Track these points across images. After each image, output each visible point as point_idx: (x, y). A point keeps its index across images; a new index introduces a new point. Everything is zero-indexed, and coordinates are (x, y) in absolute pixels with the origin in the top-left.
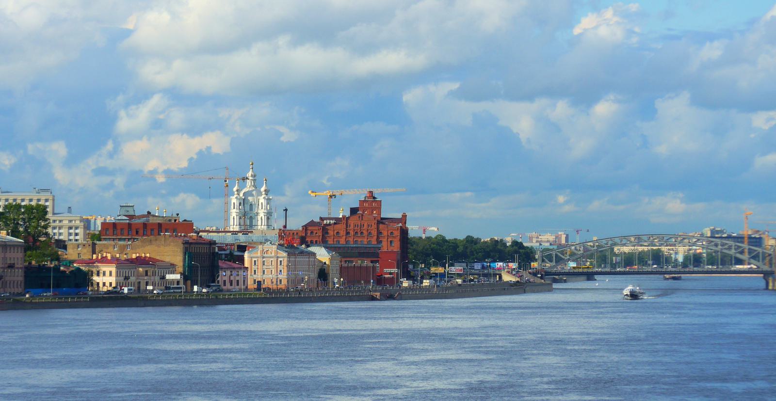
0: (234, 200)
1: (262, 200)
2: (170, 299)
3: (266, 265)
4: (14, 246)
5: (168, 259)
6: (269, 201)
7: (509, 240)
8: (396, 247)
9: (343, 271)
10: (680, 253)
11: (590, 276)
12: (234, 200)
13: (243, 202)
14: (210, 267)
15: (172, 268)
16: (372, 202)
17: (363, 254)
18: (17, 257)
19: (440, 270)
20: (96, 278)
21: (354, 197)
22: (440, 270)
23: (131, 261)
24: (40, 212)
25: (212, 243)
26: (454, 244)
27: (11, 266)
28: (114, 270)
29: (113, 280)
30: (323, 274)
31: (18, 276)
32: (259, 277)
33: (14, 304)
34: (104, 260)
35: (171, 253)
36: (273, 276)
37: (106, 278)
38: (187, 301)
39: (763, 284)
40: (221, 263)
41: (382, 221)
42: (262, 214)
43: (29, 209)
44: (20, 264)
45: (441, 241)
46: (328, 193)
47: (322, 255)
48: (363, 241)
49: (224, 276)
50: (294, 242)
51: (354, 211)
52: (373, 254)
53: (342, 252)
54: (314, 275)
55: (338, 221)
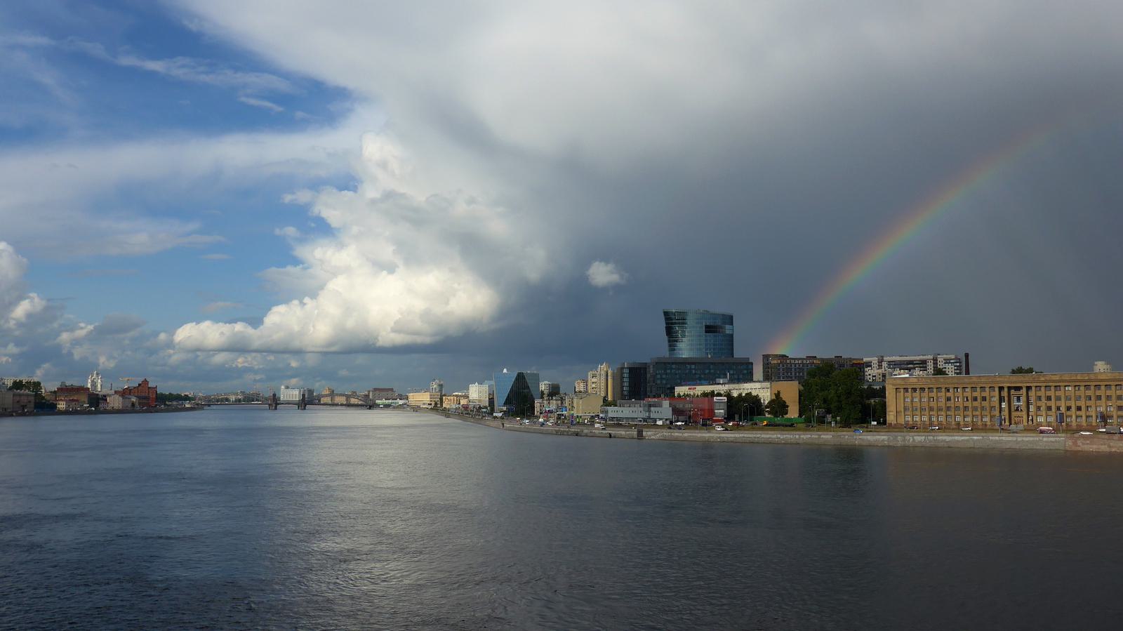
0: (89, 381)
1: (99, 381)
3: (115, 402)
4: (31, 395)
5: (83, 400)
6: (101, 381)
7: (183, 395)
8: (154, 396)
9: (139, 404)
10: (233, 398)
11: (209, 405)
12: (89, 381)
13: (92, 381)
14: (96, 402)
15: (84, 402)
16: (146, 382)
17: (145, 398)
18: (33, 398)
19: (170, 403)
20: (58, 406)
21: (140, 380)
22: (170, 403)
23: (70, 400)
25: (98, 395)
26: (165, 395)
27: (30, 402)
28: (65, 403)
29: (64, 406)
30: (133, 405)
32: (112, 405)
33: (30, 414)
34: (61, 400)
35: (84, 398)
36: (117, 405)
37: (62, 406)
38: (90, 413)
39: (268, 408)
40: (101, 401)
41: (149, 388)
42: (99, 386)
43: (34, 383)
44: (33, 401)
46: (126, 379)
48: (143, 395)
49: (101, 406)
50: (124, 393)
51: (139, 385)
54: (130, 405)
55: (135, 388)
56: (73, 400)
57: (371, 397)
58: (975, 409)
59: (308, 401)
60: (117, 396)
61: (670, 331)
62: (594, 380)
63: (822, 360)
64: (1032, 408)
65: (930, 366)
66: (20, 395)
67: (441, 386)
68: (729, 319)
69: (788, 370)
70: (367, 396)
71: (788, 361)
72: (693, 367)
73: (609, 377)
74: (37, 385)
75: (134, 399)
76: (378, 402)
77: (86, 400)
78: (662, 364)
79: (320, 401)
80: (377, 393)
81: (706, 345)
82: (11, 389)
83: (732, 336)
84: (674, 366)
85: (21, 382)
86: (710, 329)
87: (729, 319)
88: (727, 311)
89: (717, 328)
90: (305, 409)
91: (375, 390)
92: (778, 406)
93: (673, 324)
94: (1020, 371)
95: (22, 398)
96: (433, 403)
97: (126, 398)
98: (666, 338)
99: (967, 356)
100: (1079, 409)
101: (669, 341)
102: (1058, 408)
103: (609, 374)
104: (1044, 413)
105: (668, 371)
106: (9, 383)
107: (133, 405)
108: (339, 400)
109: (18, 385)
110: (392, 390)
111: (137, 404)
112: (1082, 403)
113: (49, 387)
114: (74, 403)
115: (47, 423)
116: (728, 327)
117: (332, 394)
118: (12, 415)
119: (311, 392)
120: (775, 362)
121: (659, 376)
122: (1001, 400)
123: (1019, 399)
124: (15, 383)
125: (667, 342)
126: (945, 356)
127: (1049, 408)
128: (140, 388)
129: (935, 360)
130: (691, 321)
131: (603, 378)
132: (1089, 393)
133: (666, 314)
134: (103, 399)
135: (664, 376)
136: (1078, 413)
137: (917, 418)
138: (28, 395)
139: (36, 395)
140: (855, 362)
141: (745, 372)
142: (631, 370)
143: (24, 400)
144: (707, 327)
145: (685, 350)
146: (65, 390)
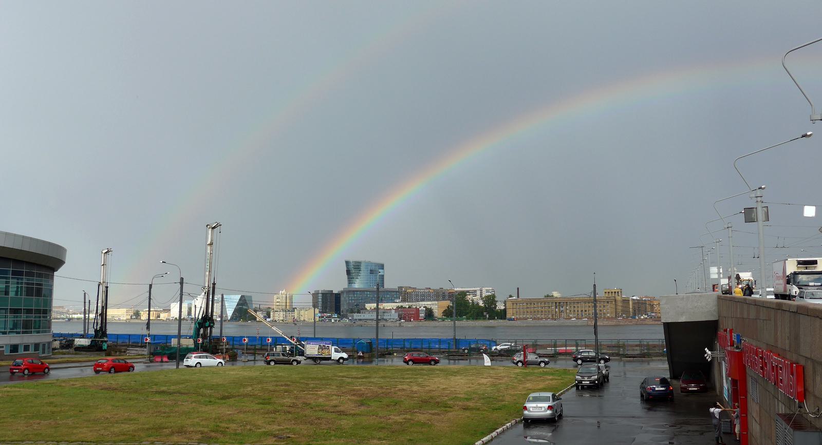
58: (545, 311)
61: (348, 272)
62: (278, 300)
63: (434, 290)
64: (568, 311)
65: (478, 293)
68: (382, 266)
69: (417, 295)
71: (417, 291)
72: (368, 293)
73: (288, 299)
78: (349, 292)
81: (370, 281)
83: (383, 276)
84: (358, 293)
86: (372, 272)
87: (382, 266)
88: (381, 262)
89: (376, 270)
92: (448, 313)
93: (352, 270)
94: (548, 296)
98: (346, 276)
99: (518, 289)
100: (586, 311)
101: (348, 278)
102: (578, 311)
103: (288, 297)
104: (573, 313)
105: (355, 295)
112: (587, 309)
116: (380, 270)
120: (410, 291)
121: (350, 298)
122: (556, 307)
123: (562, 307)
125: (347, 279)
126: (486, 288)
127: (574, 311)
129: (481, 291)
130: (363, 268)
131: (284, 299)
132: (589, 305)
133: (347, 263)
135: (353, 298)
136: (586, 313)
137: (521, 316)
140: (450, 291)
141: (395, 296)
142: (322, 294)
144: (370, 270)
145: (358, 285)
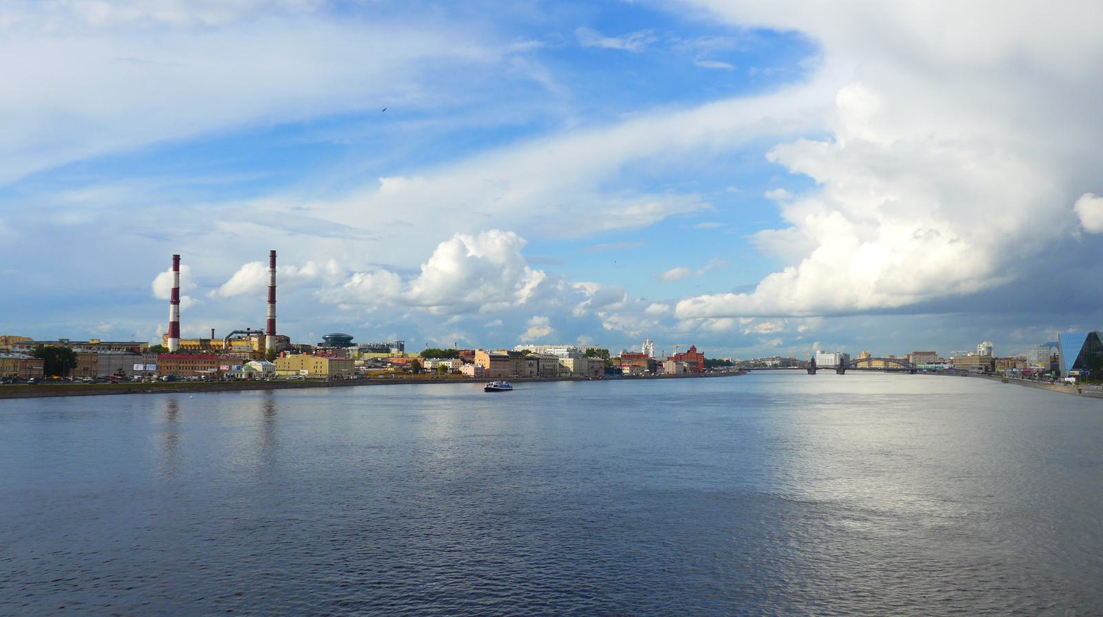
1: (651, 348)
2: (645, 378)
3: (670, 367)
8: (702, 362)
9: (691, 369)
11: (749, 370)
13: (646, 349)
14: (654, 366)
16: (694, 349)
18: (603, 364)
20: (623, 371)
24: (606, 352)
29: (628, 371)
30: (685, 370)
31: (603, 371)
34: (625, 366)
35: (644, 364)
37: (626, 371)
41: (697, 354)
43: (603, 351)
44: (603, 367)
45: (714, 360)
47: (685, 365)
48: (693, 360)
50: (678, 359)
52: (696, 364)
53: (689, 363)
55: (685, 354)
56: (635, 366)
57: (911, 361)
59: (844, 366)
60: (671, 362)
66: (594, 361)
67: (990, 348)
70: (907, 360)
74: (606, 352)
75: (685, 365)
76: (920, 366)
77: (646, 366)
79: (856, 366)
80: (918, 356)
82: (585, 356)
85: (593, 350)
90: (843, 374)
91: (916, 353)
95: (595, 364)
96: (984, 367)
97: (680, 364)
106: (584, 351)
107: (685, 370)
108: (876, 364)
109: (591, 353)
110: (934, 353)
111: (688, 369)
113: (615, 353)
114: (636, 369)
115: (616, 388)
117: (869, 359)
118: (589, 380)
119: (847, 356)
124: (588, 350)
128: (689, 354)
134: (659, 365)
138: (599, 362)
139: (606, 362)
143: (596, 366)
146: (628, 357)
